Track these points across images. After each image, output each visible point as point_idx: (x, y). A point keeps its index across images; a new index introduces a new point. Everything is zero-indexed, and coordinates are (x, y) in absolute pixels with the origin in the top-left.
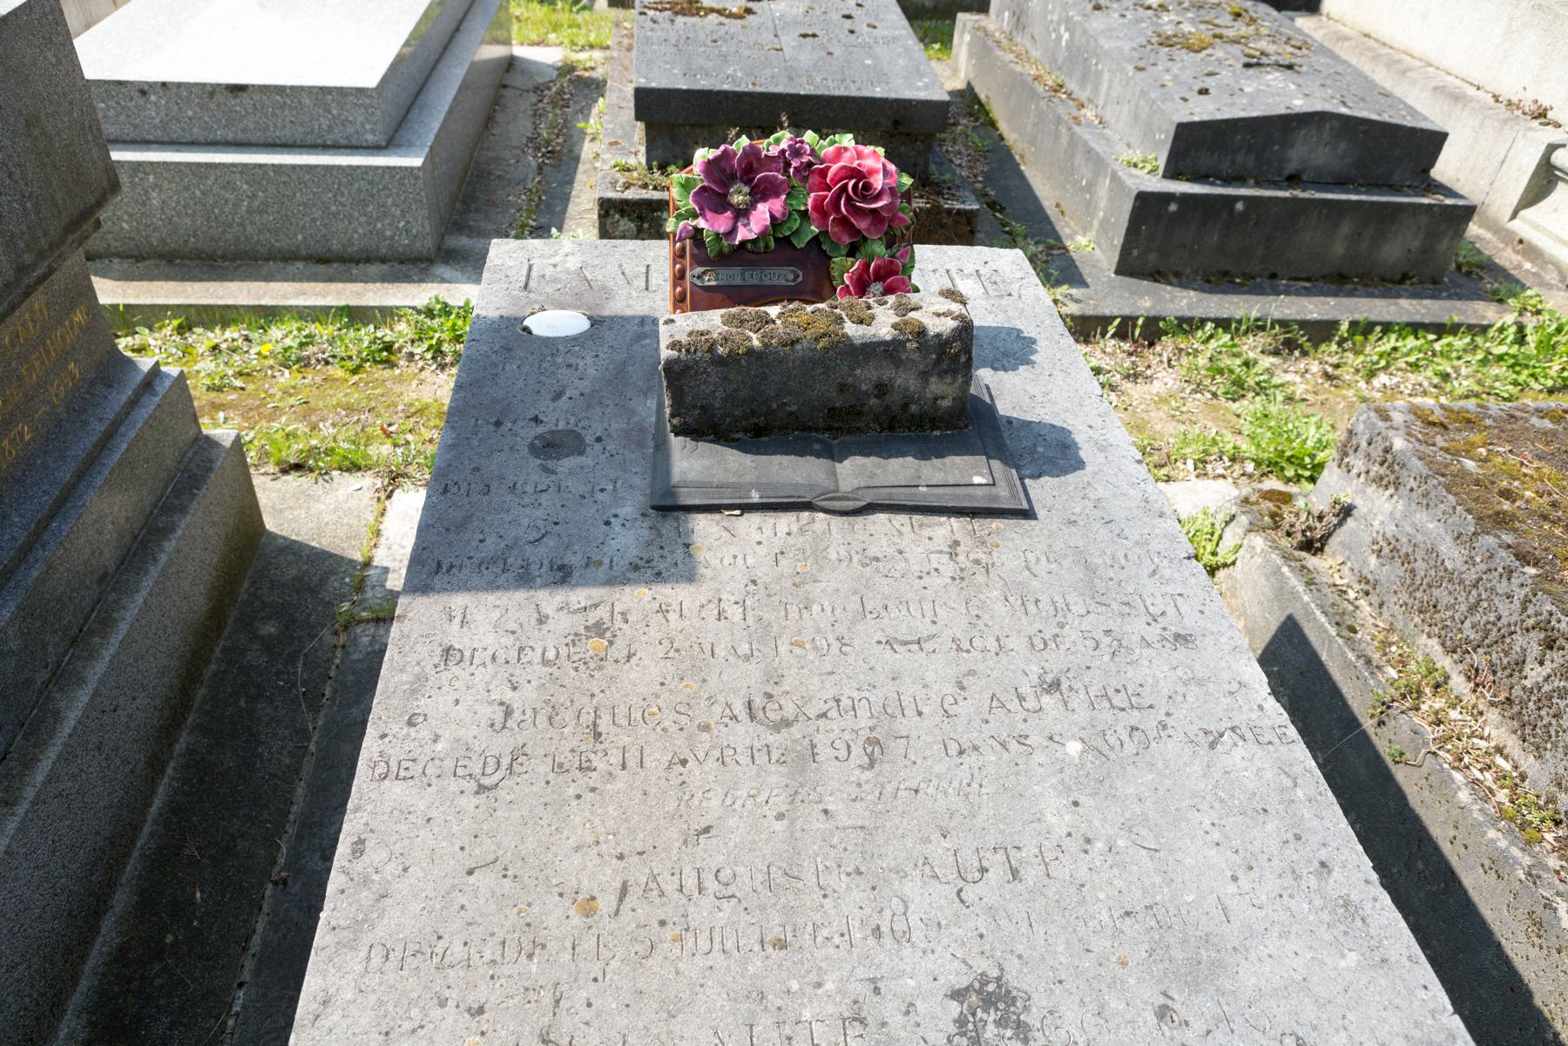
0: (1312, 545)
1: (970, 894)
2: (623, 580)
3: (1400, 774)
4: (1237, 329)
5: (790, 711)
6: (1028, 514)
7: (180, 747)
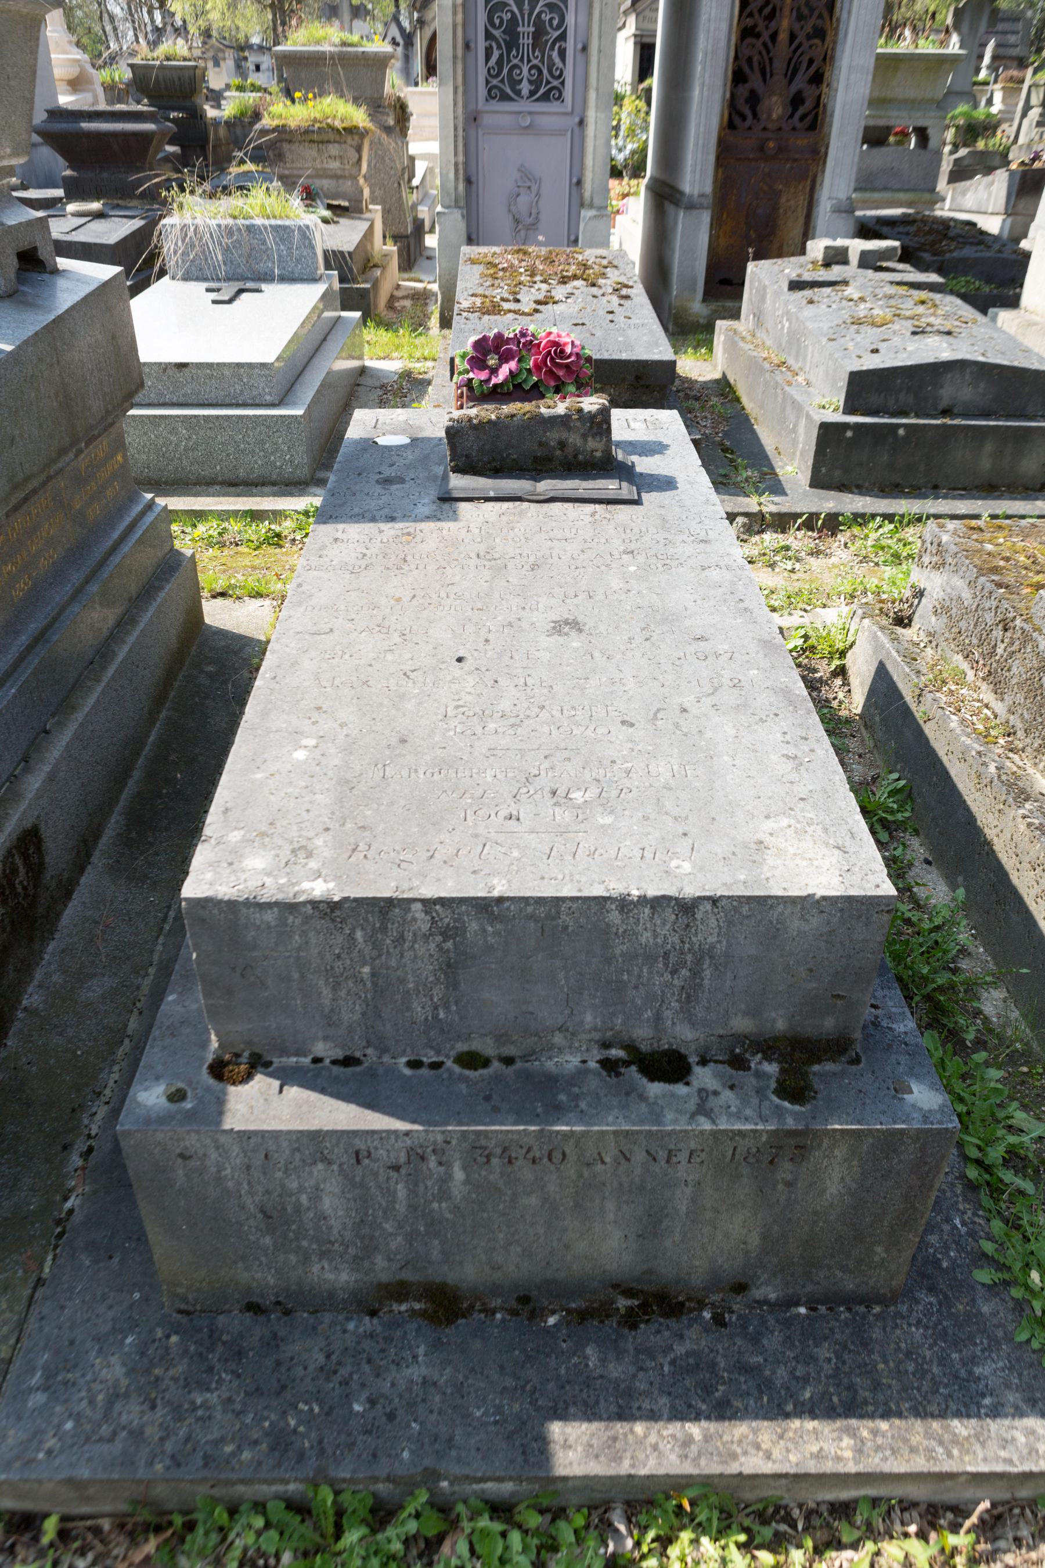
0: (902, 621)
1: (568, 601)
2: (422, 521)
3: (929, 729)
4: (901, 522)
5: (497, 556)
6: (637, 502)
7: (163, 714)
